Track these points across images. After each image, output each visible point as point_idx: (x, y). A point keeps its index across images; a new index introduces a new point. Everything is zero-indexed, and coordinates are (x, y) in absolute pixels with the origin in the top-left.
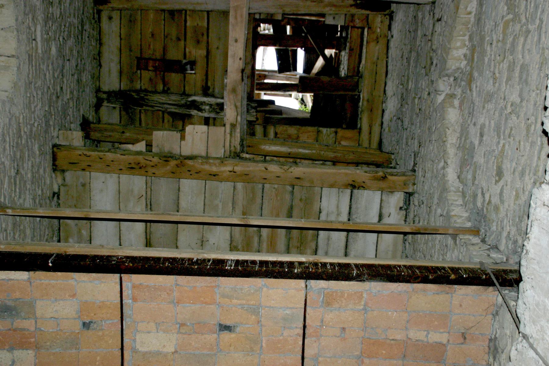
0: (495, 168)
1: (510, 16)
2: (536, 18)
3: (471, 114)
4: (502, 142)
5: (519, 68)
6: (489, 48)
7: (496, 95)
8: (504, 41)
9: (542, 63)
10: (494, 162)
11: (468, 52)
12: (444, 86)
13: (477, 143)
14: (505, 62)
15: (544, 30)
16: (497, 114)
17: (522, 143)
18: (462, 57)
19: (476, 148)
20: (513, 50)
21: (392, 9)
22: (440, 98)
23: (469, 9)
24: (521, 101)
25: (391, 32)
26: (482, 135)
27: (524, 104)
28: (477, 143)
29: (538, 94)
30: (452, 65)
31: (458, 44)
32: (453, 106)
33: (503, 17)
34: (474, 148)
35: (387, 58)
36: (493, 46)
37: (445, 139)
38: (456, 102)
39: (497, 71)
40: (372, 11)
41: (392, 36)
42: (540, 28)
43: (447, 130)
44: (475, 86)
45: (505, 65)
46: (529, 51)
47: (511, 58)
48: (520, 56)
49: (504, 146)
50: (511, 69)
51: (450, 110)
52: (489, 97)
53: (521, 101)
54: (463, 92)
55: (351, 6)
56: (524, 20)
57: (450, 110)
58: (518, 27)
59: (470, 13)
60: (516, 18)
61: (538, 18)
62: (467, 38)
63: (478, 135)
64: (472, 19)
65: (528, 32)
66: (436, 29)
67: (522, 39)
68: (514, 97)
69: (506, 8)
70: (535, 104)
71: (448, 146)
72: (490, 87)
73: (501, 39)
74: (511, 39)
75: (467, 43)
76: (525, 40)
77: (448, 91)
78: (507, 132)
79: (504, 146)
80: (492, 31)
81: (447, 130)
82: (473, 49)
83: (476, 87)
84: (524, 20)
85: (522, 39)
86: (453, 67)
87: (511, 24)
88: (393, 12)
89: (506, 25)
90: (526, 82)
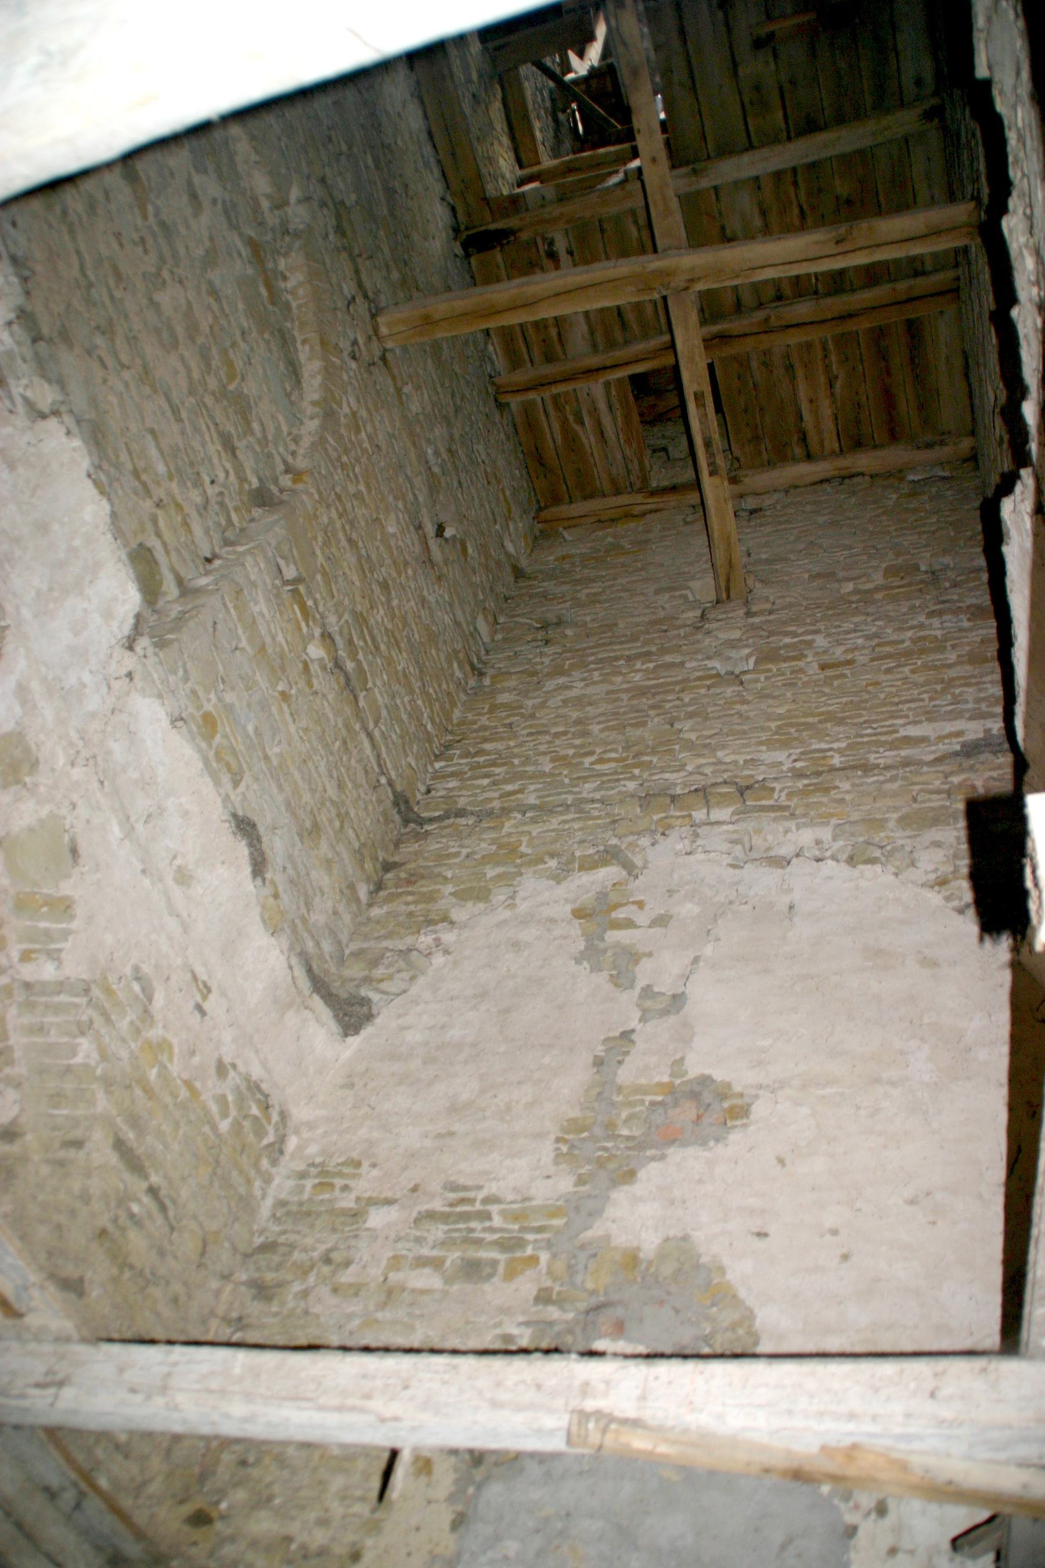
0: (142, 174)
1: (232, 387)
2: (189, 419)
3: (229, 212)
4: (152, 220)
5: (181, 340)
6: (245, 324)
7: (198, 272)
8: (224, 353)
9: (146, 373)
10: (149, 179)
11: (282, 285)
12: (298, 215)
13: (197, 179)
14: (207, 330)
15: (169, 414)
16: (182, 251)
17: (117, 247)
18: (288, 274)
19: (193, 172)
20: (205, 357)
21: (458, 244)
22: (295, 194)
23: (307, 347)
24: (151, 300)
25: (449, 204)
26: (194, 196)
27: (145, 302)
28: (197, 179)
29: (130, 331)
30: (296, 258)
31: (301, 292)
32: (268, 197)
33: (243, 379)
34: (195, 167)
35: (439, 161)
36: (238, 333)
37: (254, 143)
38: (265, 204)
39: (215, 306)
40: (486, 232)
41: (443, 199)
42: (175, 411)
43: (258, 159)
44: (244, 254)
45: (204, 327)
46: (176, 372)
47: (200, 340)
48: (186, 354)
49: (145, 217)
50: (193, 330)
51: (269, 190)
52: (210, 259)
53: (151, 300)
54: (262, 224)
55: (521, 230)
56: (209, 400)
57: (269, 190)
58: (212, 383)
59: (304, 342)
60: (222, 394)
61: (186, 422)
62: (294, 304)
63: (199, 192)
64: (296, 333)
65: (192, 392)
66: (353, 284)
67: (196, 375)
68: (164, 298)
69: (245, 391)
70: (126, 317)
71: (244, 137)
72: (215, 276)
73: (231, 351)
74: (214, 363)
75: (290, 297)
76: (190, 377)
77: (289, 210)
78: (150, 241)
79: (145, 217)
80: (252, 350)
81: (258, 159)
82: (274, 296)
83: (240, 255)
84: (209, 400)
85: (196, 375)
86: (293, 254)
87: (225, 382)
88: (455, 239)
89: (232, 377)
90: (158, 331)
